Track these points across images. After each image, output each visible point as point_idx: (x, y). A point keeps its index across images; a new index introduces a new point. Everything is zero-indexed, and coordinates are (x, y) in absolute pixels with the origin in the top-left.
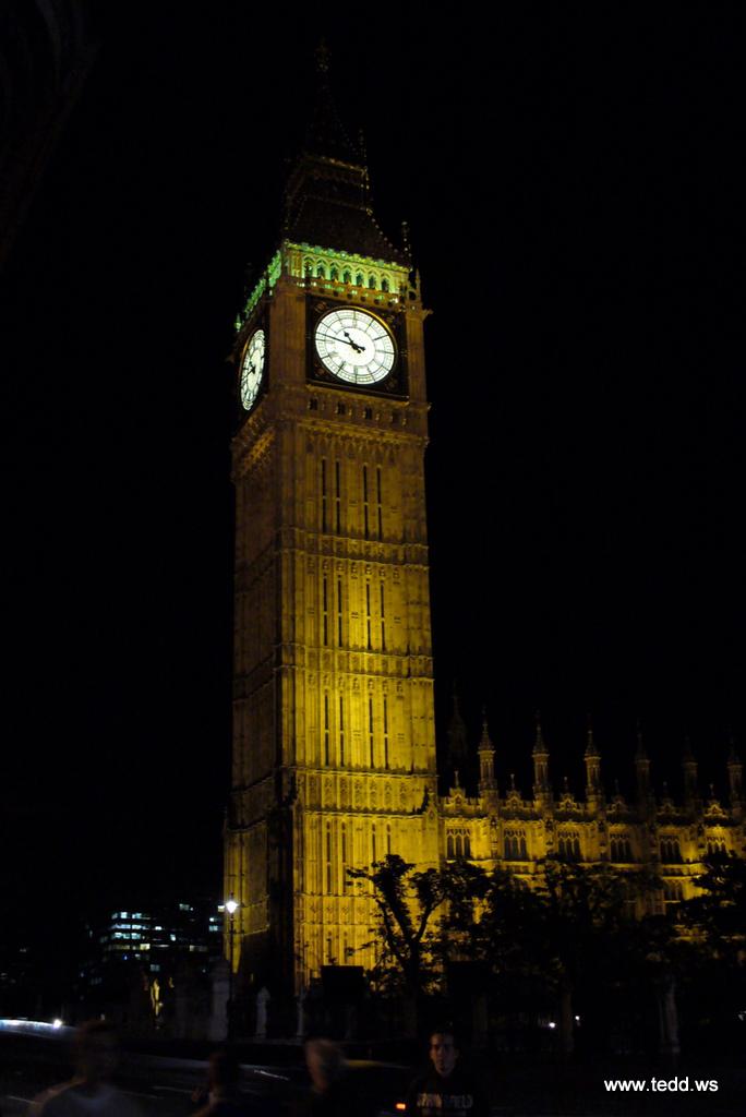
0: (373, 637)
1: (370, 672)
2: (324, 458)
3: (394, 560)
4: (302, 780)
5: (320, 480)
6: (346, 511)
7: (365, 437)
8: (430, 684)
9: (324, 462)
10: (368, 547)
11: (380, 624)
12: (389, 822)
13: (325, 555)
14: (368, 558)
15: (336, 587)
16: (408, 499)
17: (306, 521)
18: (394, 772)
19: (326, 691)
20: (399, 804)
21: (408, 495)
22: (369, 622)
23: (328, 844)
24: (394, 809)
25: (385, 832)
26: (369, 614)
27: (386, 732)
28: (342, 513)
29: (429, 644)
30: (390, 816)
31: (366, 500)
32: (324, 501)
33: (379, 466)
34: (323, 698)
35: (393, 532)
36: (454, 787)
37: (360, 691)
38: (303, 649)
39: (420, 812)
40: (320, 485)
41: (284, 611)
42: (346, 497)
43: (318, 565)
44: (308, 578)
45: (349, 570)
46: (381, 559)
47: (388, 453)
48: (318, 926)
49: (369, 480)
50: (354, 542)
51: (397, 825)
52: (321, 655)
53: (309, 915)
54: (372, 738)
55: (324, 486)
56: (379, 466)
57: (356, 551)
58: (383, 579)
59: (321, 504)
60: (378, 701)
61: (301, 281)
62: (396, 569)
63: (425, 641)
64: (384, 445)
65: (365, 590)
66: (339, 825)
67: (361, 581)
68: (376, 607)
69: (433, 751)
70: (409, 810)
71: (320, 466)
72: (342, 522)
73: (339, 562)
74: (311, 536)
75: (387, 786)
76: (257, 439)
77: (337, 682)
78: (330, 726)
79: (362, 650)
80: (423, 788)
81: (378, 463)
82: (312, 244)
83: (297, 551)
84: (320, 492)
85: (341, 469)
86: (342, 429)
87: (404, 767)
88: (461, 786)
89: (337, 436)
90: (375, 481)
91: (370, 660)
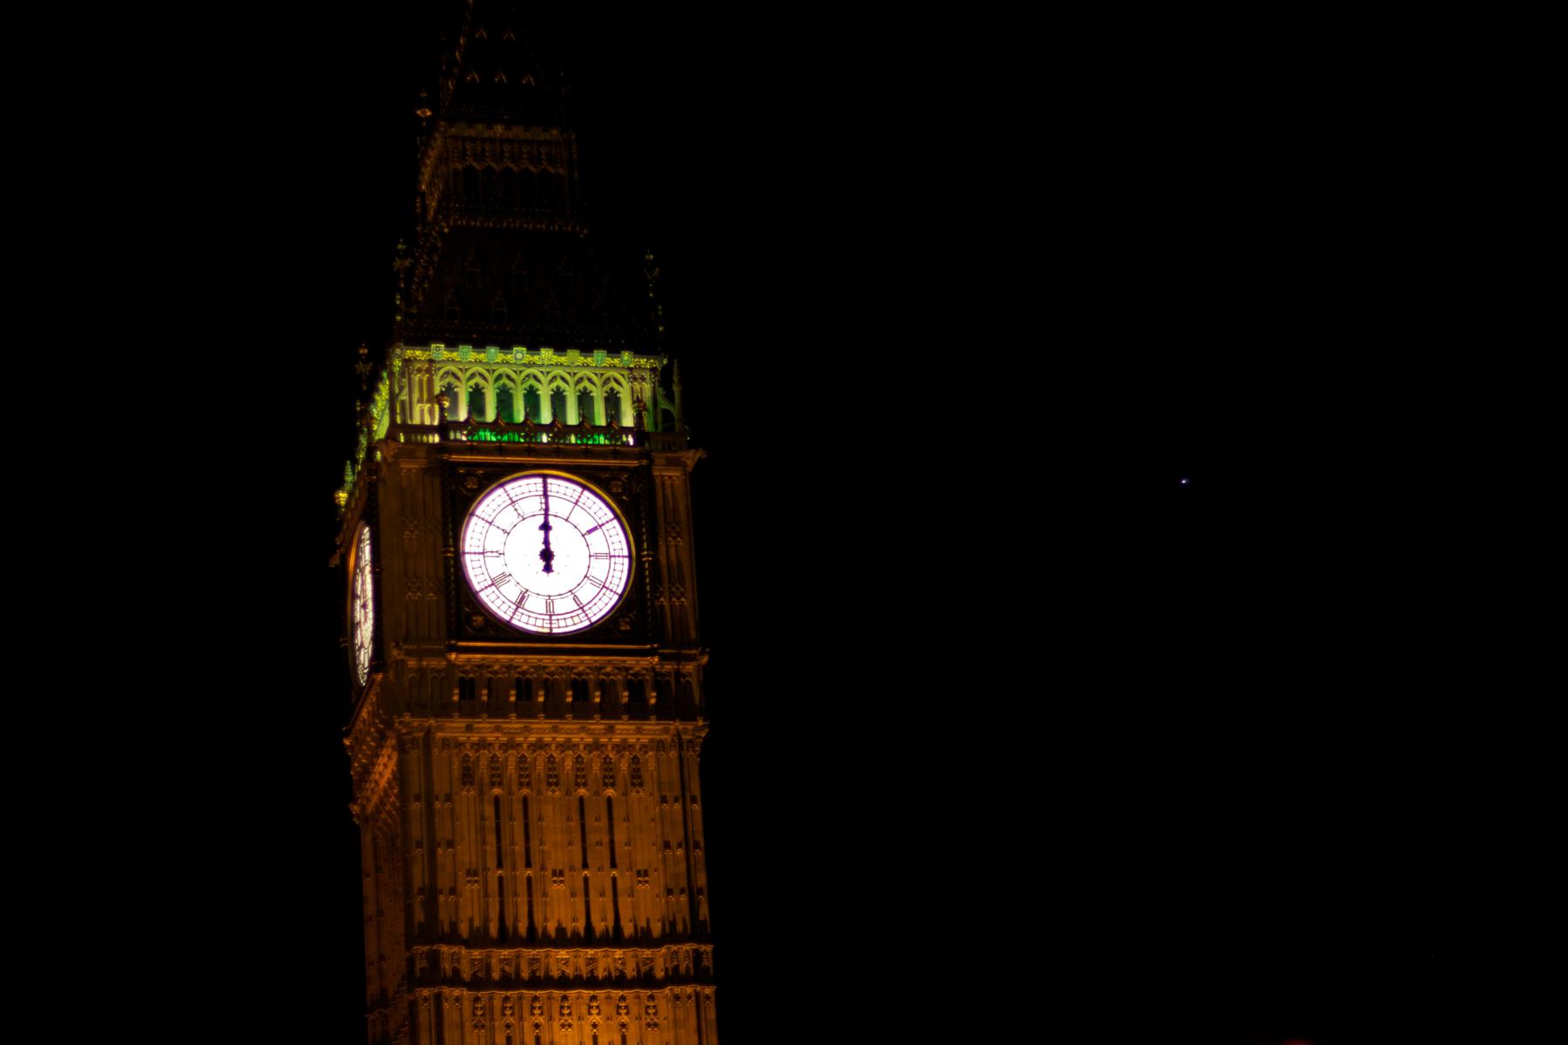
6: (545, 894)
10: (592, 960)
14: (592, 982)
16: (668, 852)
31: (585, 866)
33: (610, 792)
35: (644, 924)
40: (491, 848)
42: (543, 868)
45: (556, 1015)
47: (624, 766)
50: (563, 954)
55: (499, 849)
56: (610, 792)
59: (493, 886)
61: (430, 430)
62: (652, 998)
67: (581, 1028)
71: (489, 810)
72: (538, 918)
73: (535, 999)
82: (452, 344)
83: (446, 990)
84: (492, 862)
85: (533, 811)
86: (527, 730)
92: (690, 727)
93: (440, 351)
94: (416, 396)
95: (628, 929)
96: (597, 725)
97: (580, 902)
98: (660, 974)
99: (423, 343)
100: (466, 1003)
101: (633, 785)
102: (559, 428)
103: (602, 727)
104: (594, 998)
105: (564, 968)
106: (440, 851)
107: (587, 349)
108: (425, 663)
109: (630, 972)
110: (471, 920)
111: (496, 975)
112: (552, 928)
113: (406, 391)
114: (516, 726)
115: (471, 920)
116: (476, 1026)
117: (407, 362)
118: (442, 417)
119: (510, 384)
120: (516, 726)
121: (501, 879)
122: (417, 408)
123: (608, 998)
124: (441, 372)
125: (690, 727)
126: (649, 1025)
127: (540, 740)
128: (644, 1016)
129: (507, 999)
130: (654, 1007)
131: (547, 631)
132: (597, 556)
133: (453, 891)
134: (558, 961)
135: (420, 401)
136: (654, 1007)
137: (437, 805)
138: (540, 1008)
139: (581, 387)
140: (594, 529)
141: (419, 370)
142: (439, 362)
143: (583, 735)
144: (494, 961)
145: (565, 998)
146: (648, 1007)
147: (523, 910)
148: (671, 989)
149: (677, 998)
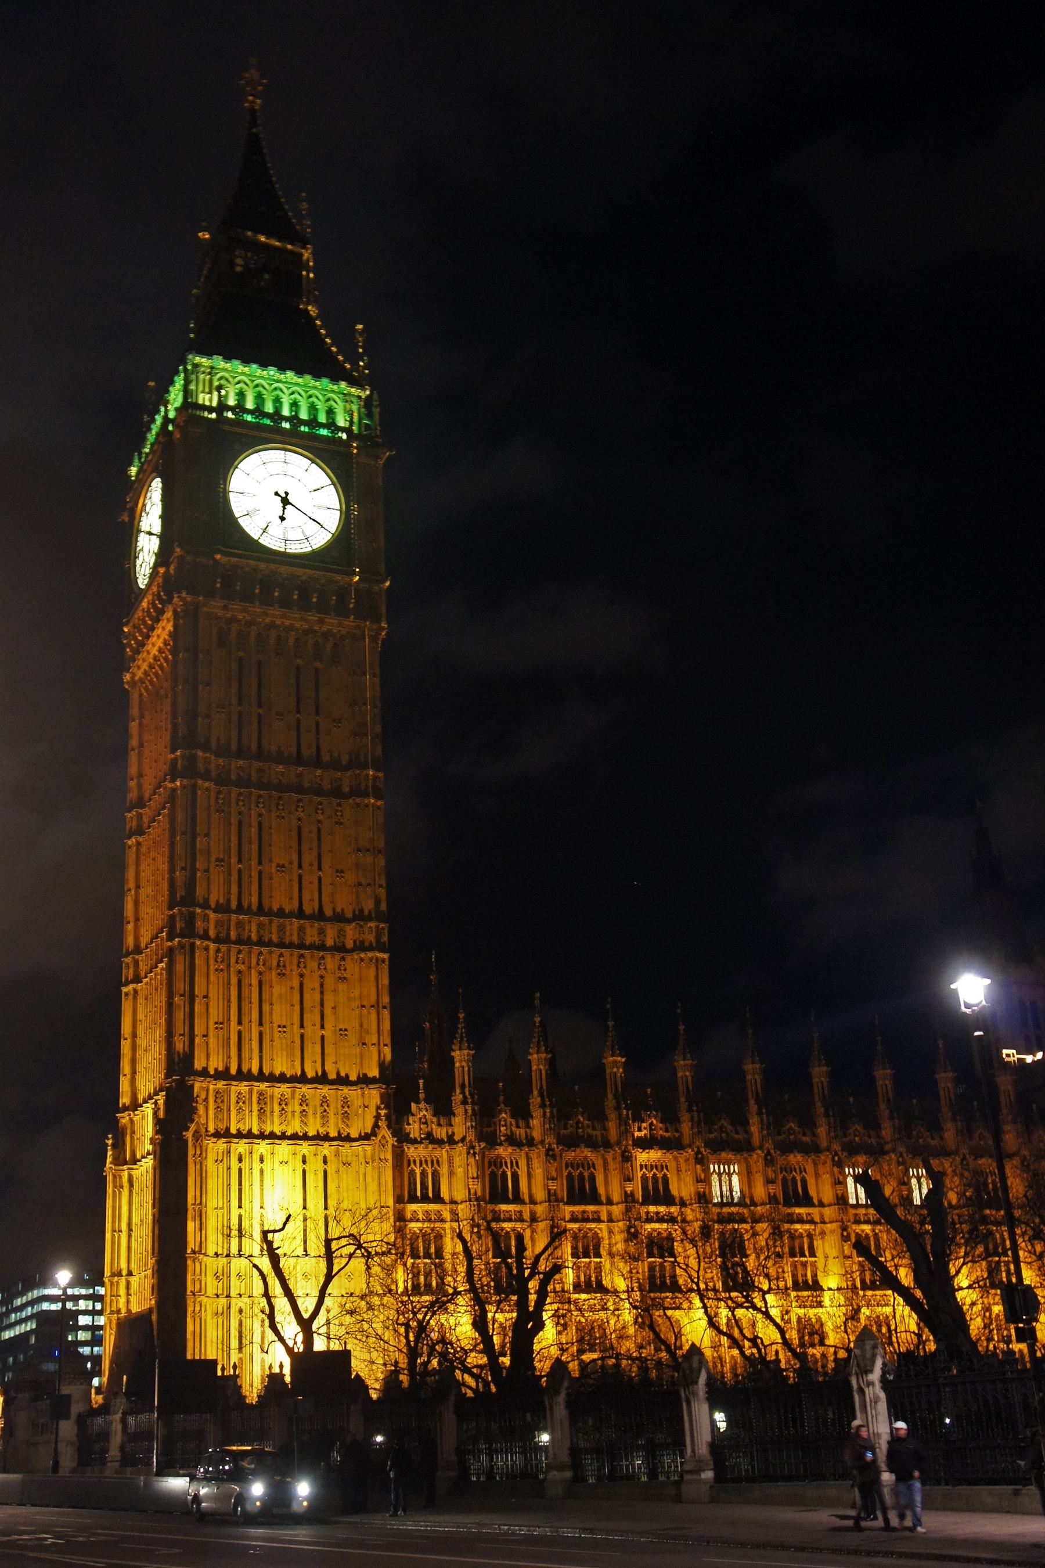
0: (306, 897)
2: (240, 654)
4: (203, 1096)
7: (297, 625)
8: (383, 961)
9: (240, 661)
10: (301, 775)
11: (316, 881)
12: (326, 1152)
13: (259, 789)
14: (299, 789)
15: (254, 831)
17: (213, 741)
18: (331, 1082)
19: (240, 972)
20: (341, 1125)
22: (300, 877)
23: (240, 1184)
25: (321, 1167)
26: (300, 866)
27: (322, 1027)
29: (383, 907)
30: (327, 1144)
31: (298, 711)
33: (318, 665)
34: (234, 980)
35: (336, 755)
37: (287, 972)
38: (206, 915)
43: (230, 802)
44: (215, 816)
46: (318, 791)
47: (329, 647)
48: (223, 1301)
50: (280, 768)
51: (337, 1154)
52: (233, 924)
53: (211, 1285)
54: (302, 1036)
55: (240, 692)
56: (318, 665)
58: (321, 817)
60: (312, 983)
61: (211, 410)
62: (339, 805)
63: (378, 901)
64: (326, 635)
65: (295, 833)
66: (256, 1157)
68: (309, 857)
73: (260, 796)
75: (324, 1101)
76: (153, 629)
77: (254, 961)
78: (245, 1020)
79: (291, 915)
82: (228, 358)
84: (234, 701)
86: (265, 614)
88: (427, 1101)
91: (302, 929)
92: (375, 627)
93: (219, 362)
94: (201, 388)
95: (326, 757)
96: (313, 617)
98: (346, 790)
99: (209, 354)
100: (212, 793)
102: (295, 420)
104: (300, 800)
105: (281, 778)
106: (200, 687)
107: (317, 376)
109: (326, 786)
110: (218, 739)
111: (233, 777)
112: (274, 748)
113: (194, 383)
114: (258, 610)
115: (218, 739)
116: (218, 811)
117: (196, 366)
118: (220, 401)
119: (264, 392)
120: (258, 610)
121: (240, 712)
122: (201, 396)
123: (310, 801)
124: (218, 376)
126: (337, 823)
127: (273, 622)
129: (240, 794)
130: (341, 811)
131: (283, 550)
133: (208, 716)
134: (277, 772)
135: (203, 392)
136: (341, 811)
137: (201, 656)
138: (263, 803)
139: (311, 400)
141: (204, 373)
142: (217, 369)
143: (303, 623)
144: (233, 767)
145: (280, 798)
146: (337, 810)
147: (255, 736)
148: (354, 800)
149: (358, 805)
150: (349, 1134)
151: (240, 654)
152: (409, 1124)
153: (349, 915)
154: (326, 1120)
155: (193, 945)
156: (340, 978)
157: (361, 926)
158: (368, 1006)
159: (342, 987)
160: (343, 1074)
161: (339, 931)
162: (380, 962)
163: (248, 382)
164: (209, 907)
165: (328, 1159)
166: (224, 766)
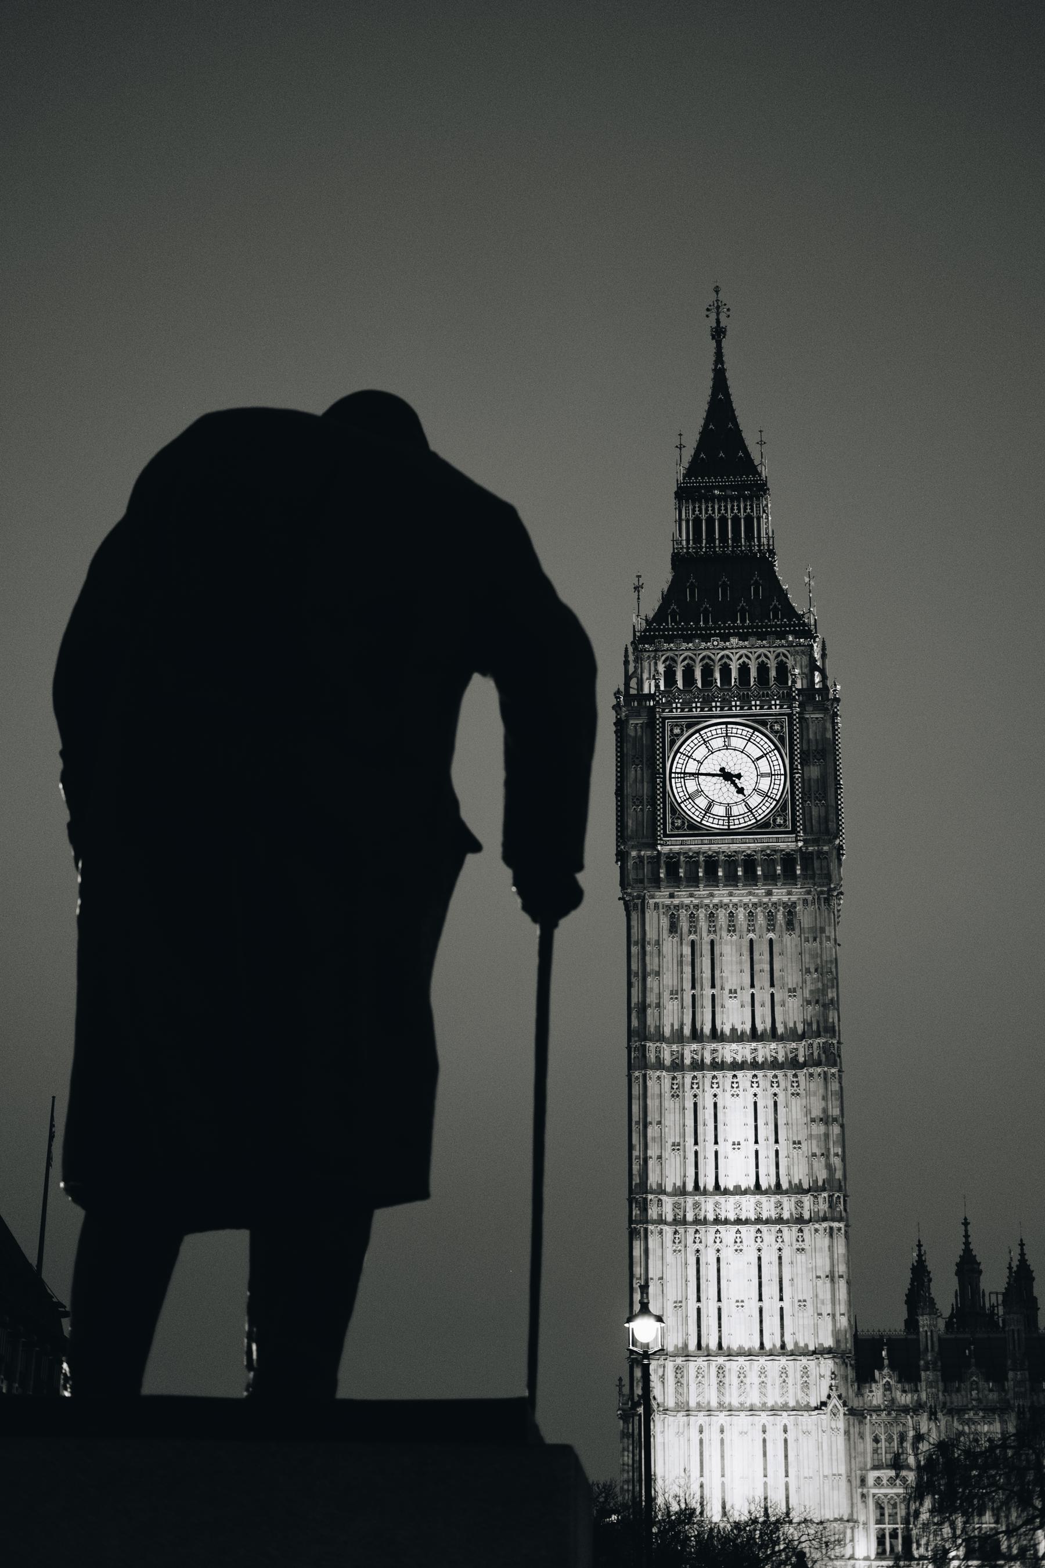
1: (759, 1221)
2: (692, 937)
3: (793, 1064)
5: (687, 969)
8: (839, 1229)
9: (693, 943)
14: (755, 1065)
20: (800, 1395)
21: (808, 971)
24: (792, 1403)
28: (718, 1009)
30: (785, 1414)
31: (752, 986)
32: (694, 996)
36: (881, 1368)
38: (660, 1200)
39: (824, 1404)
41: (635, 1153)
42: (722, 988)
49: (756, 957)
56: (771, 935)
57: (739, 1059)
58: (777, 1090)
60: (769, 1257)
69: (843, 1322)
70: (813, 1404)
71: (687, 950)
74: (675, 1047)
75: (784, 1371)
79: (746, 1192)
80: (829, 1373)
81: (769, 930)
84: (687, 985)
87: (806, 1345)
89: (707, 905)
90: (766, 956)
91: (758, 1204)
97: (748, 1010)
101: (788, 930)
103: (763, 891)
105: (735, 1056)
108: (643, 853)
110: (672, 1025)
115: (672, 1025)
116: (673, 1096)
125: (825, 889)
126: (793, 1094)
128: (789, 1088)
132: (762, 775)
135: (648, 679)
140: (762, 757)
143: (751, 897)
144: (685, 1052)
146: (793, 1082)
149: (811, 1075)
150: (809, 1403)
151: (692, 937)
152: (871, 1391)
153: (806, 1186)
154: (785, 1390)
155: (646, 1229)
156: (798, 1250)
157: (815, 1197)
158: (823, 1276)
159: (801, 1258)
160: (802, 1344)
161: (796, 1203)
162: (835, 1231)
163: (694, 657)
164: (664, 1192)
165: (788, 1428)
166: (678, 1051)
